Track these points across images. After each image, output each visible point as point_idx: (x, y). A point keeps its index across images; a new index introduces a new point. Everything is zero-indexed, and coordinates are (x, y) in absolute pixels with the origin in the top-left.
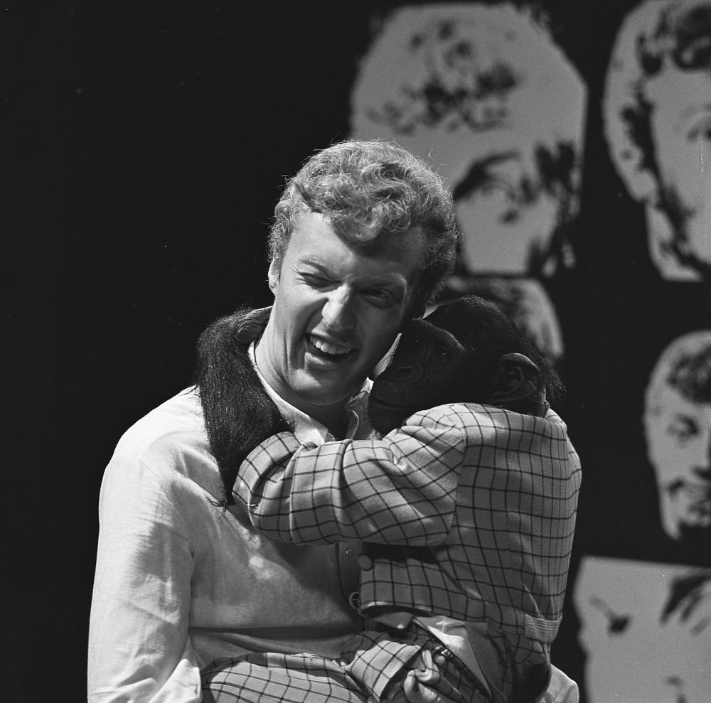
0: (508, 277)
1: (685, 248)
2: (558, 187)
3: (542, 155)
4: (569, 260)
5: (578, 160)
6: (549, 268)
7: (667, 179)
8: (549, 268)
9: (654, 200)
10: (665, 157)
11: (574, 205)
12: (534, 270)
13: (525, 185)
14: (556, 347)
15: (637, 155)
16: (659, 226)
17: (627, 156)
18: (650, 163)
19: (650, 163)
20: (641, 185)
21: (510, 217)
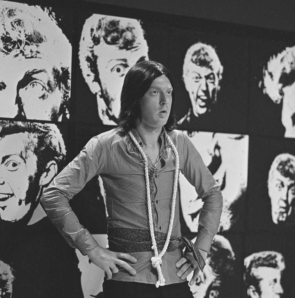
0: (43, 122)
1: (111, 113)
2: (62, 85)
3: (55, 71)
4: (68, 116)
5: (70, 75)
6: (60, 119)
7: (104, 88)
8: (60, 119)
9: (100, 93)
10: (101, 77)
11: (69, 95)
12: (54, 120)
13: (49, 84)
14: (64, 152)
15: (93, 75)
16: (101, 104)
17: (88, 75)
18: (97, 79)
19: (97, 79)
20: (94, 88)
21: (43, 97)
